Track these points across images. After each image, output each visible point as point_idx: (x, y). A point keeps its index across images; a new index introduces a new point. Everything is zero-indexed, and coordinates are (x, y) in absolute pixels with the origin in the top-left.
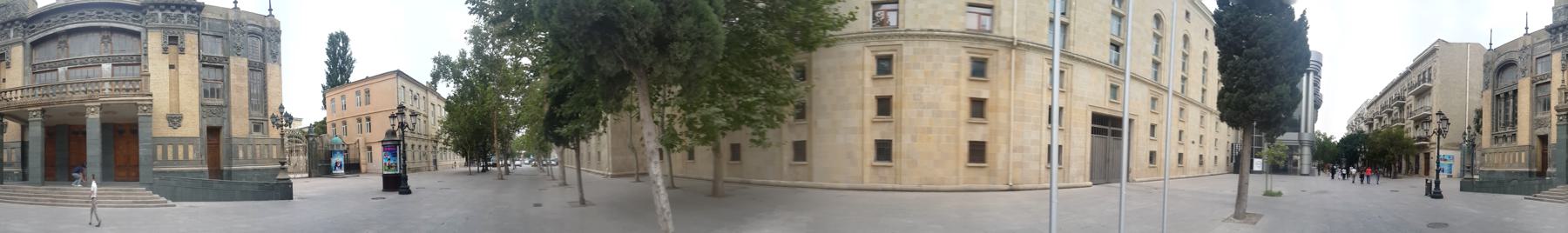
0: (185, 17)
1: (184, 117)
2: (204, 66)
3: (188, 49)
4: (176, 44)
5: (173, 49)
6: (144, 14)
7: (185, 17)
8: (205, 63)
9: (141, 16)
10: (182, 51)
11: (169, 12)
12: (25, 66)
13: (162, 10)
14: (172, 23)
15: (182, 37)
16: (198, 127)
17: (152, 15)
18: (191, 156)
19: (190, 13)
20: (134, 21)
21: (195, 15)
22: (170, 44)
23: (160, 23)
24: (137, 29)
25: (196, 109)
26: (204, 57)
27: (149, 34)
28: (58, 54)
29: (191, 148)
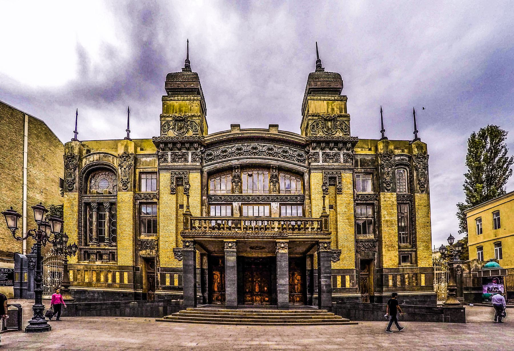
0: (342, 156)
1: (342, 252)
2: (358, 204)
3: (344, 190)
4: (334, 185)
5: (332, 190)
6: (307, 153)
7: (342, 156)
8: (359, 202)
9: (305, 156)
10: (339, 191)
11: (328, 151)
12: (202, 197)
13: (322, 149)
14: (330, 164)
15: (340, 178)
16: (354, 260)
17: (314, 154)
18: (348, 285)
19: (345, 151)
20: (298, 160)
21: (350, 152)
22: (330, 185)
23: (321, 163)
24: (301, 169)
25: (352, 245)
26: (358, 196)
27: (312, 174)
28: (233, 188)
29: (348, 278)
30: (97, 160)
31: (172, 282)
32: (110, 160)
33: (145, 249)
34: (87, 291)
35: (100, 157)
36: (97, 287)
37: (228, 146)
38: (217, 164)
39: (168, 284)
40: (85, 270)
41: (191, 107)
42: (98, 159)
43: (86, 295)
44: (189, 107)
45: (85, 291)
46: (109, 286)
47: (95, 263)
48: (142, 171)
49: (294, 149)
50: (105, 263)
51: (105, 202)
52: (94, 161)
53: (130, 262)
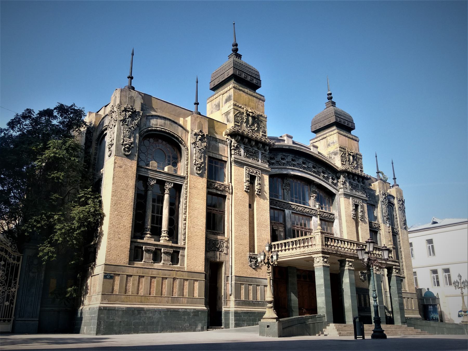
30: (161, 126)
31: (247, 294)
32: (179, 132)
33: (213, 251)
34: (142, 309)
35: (165, 123)
36: (156, 302)
37: (284, 154)
38: (277, 169)
39: (243, 298)
40: (139, 276)
41: (257, 105)
42: (163, 125)
43: (141, 317)
44: (256, 104)
45: (140, 310)
46: (175, 300)
47: (152, 266)
48: (211, 156)
49: (329, 172)
50: (168, 267)
51: (168, 182)
52: (157, 125)
53: (201, 268)
